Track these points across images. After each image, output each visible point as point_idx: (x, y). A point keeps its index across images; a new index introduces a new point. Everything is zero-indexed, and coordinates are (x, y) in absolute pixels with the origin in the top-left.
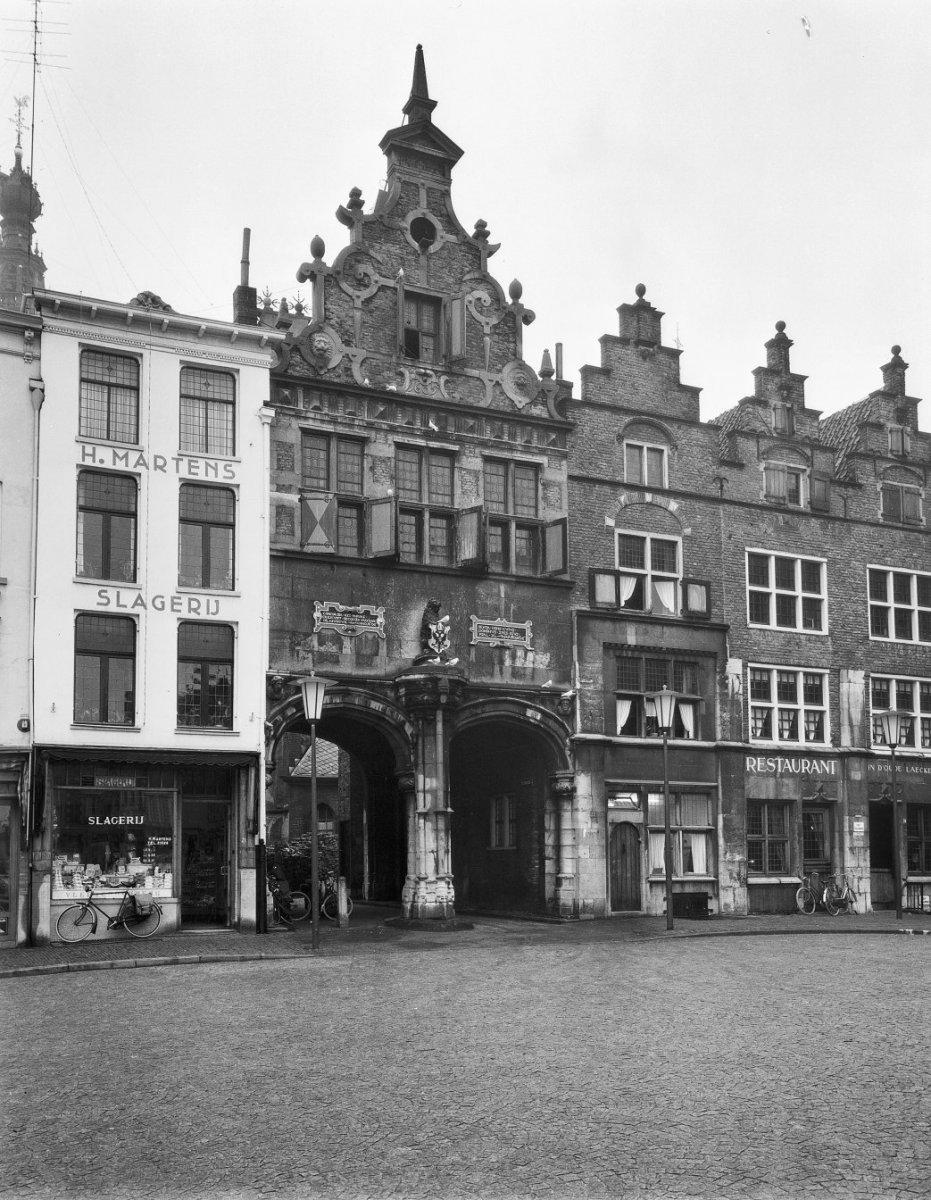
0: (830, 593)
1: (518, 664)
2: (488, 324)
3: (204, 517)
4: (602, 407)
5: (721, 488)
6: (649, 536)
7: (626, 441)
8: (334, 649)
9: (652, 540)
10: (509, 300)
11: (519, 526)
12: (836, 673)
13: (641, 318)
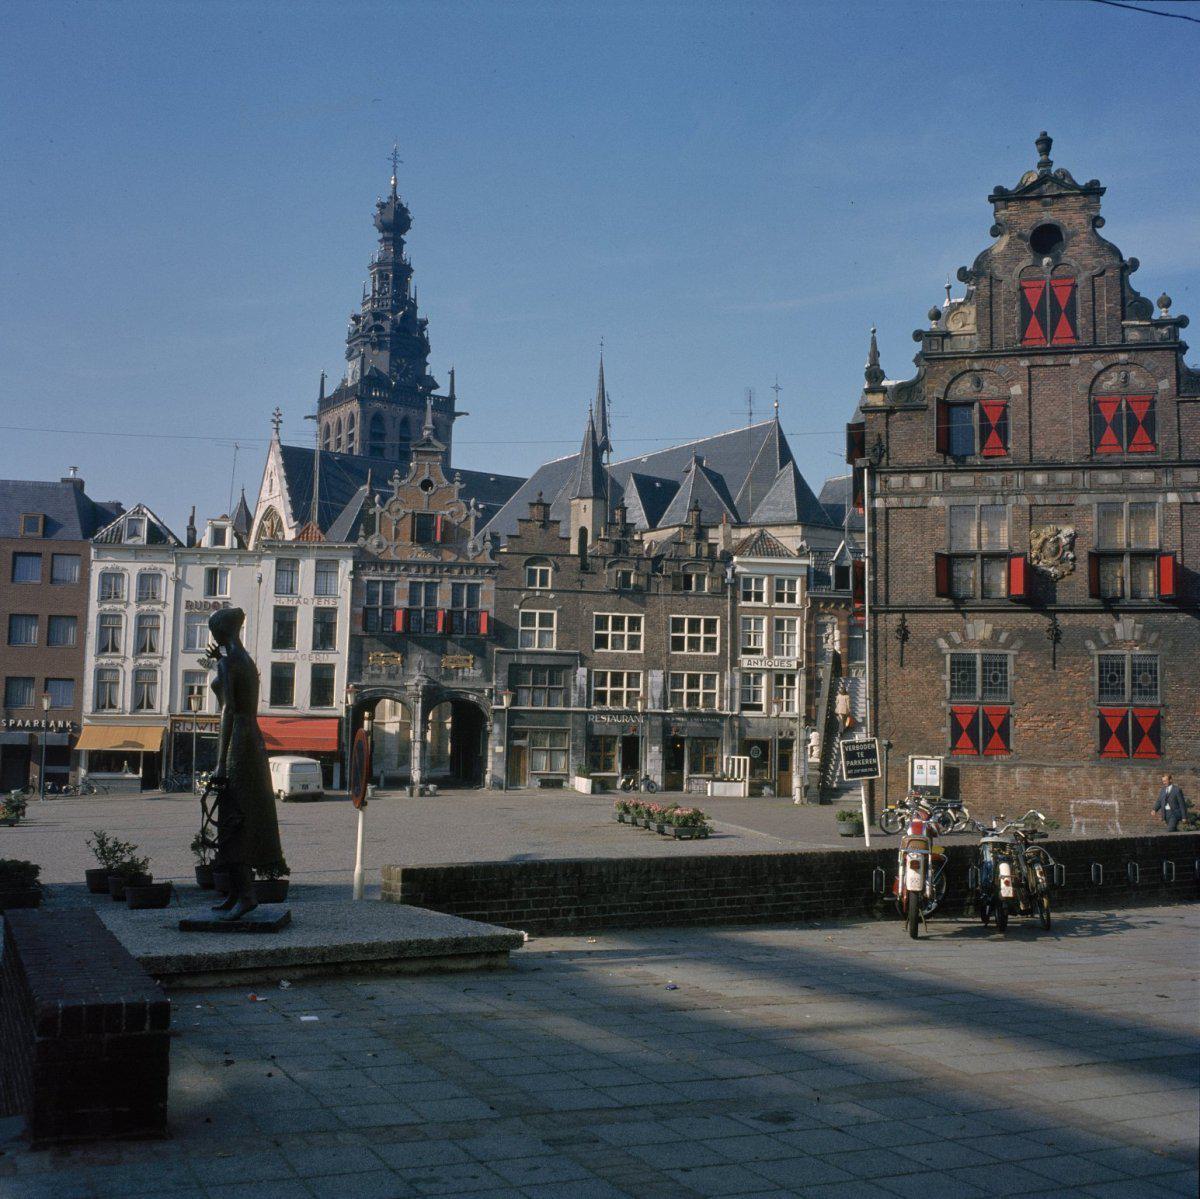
0: (645, 631)
1: (466, 674)
6: (538, 612)
8: (378, 672)
12: (646, 672)
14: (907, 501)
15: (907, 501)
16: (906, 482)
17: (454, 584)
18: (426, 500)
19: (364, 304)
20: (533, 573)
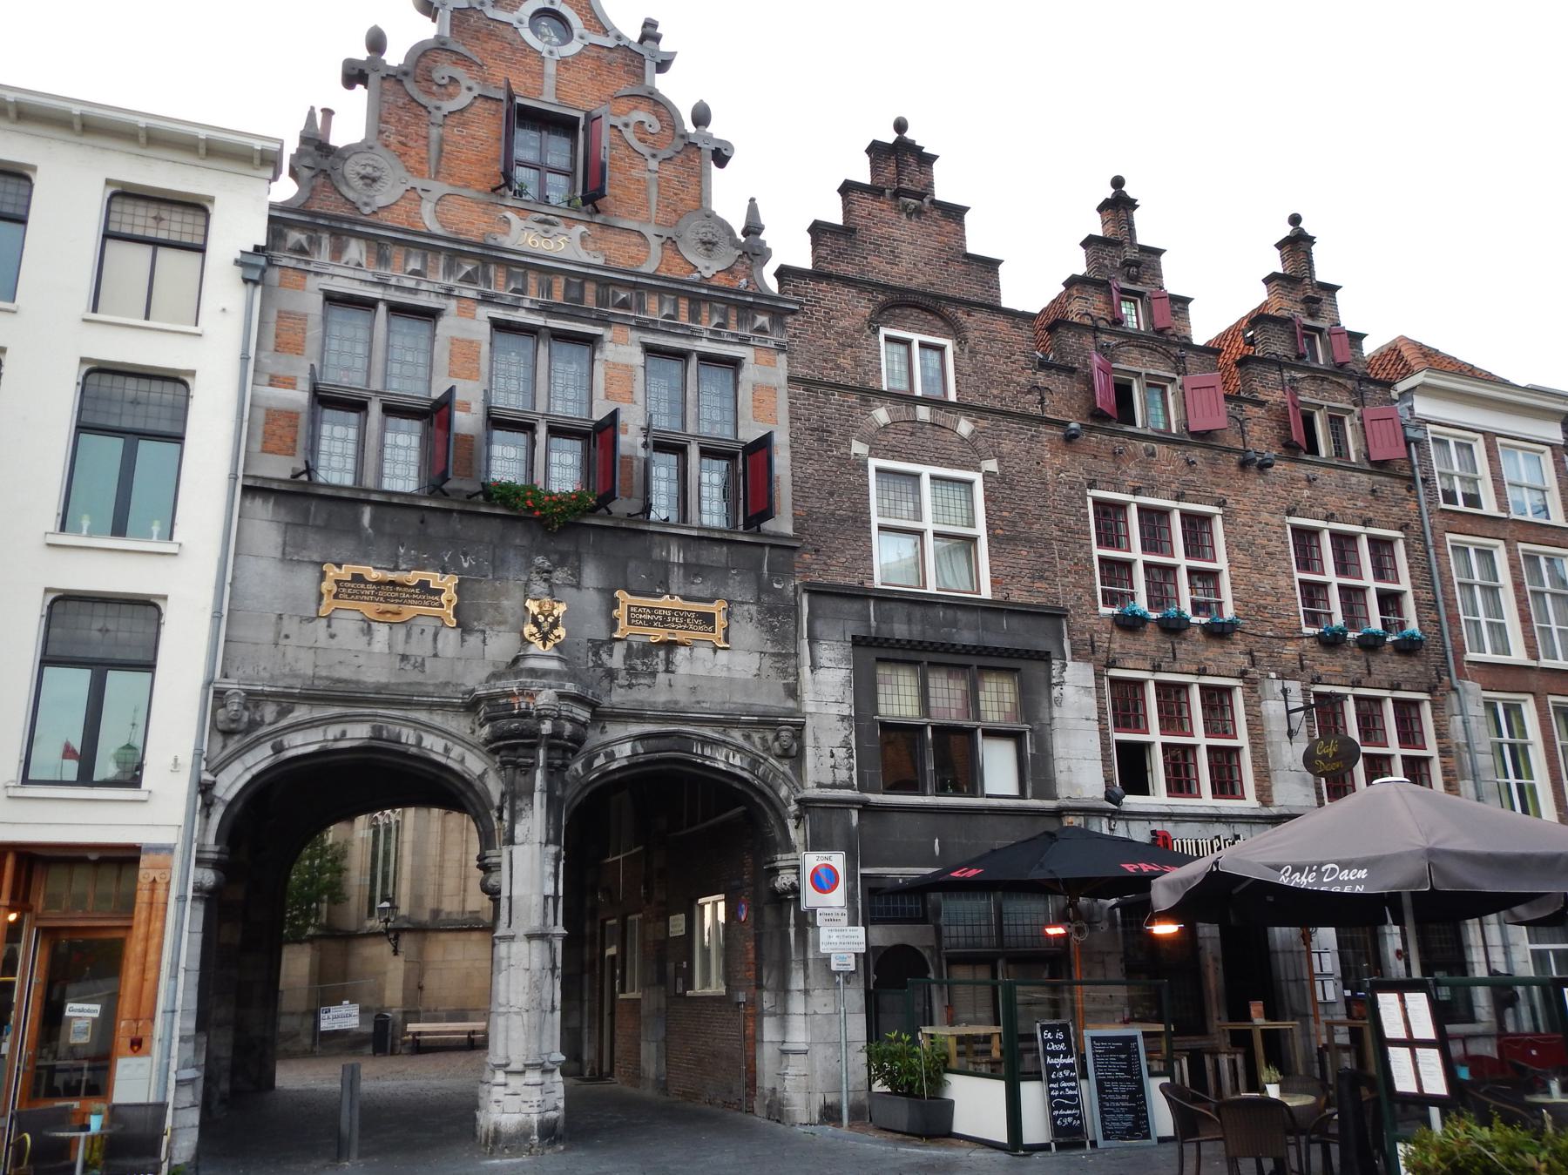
2: (654, 156)
3: (127, 423)
4: (847, 281)
5: (1042, 402)
6: (926, 471)
7: (883, 331)
9: (933, 478)
10: (690, 128)
11: (705, 452)
12: (1252, 685)
13: (900, 163)
17: (650, 350)
18: (550, 68)
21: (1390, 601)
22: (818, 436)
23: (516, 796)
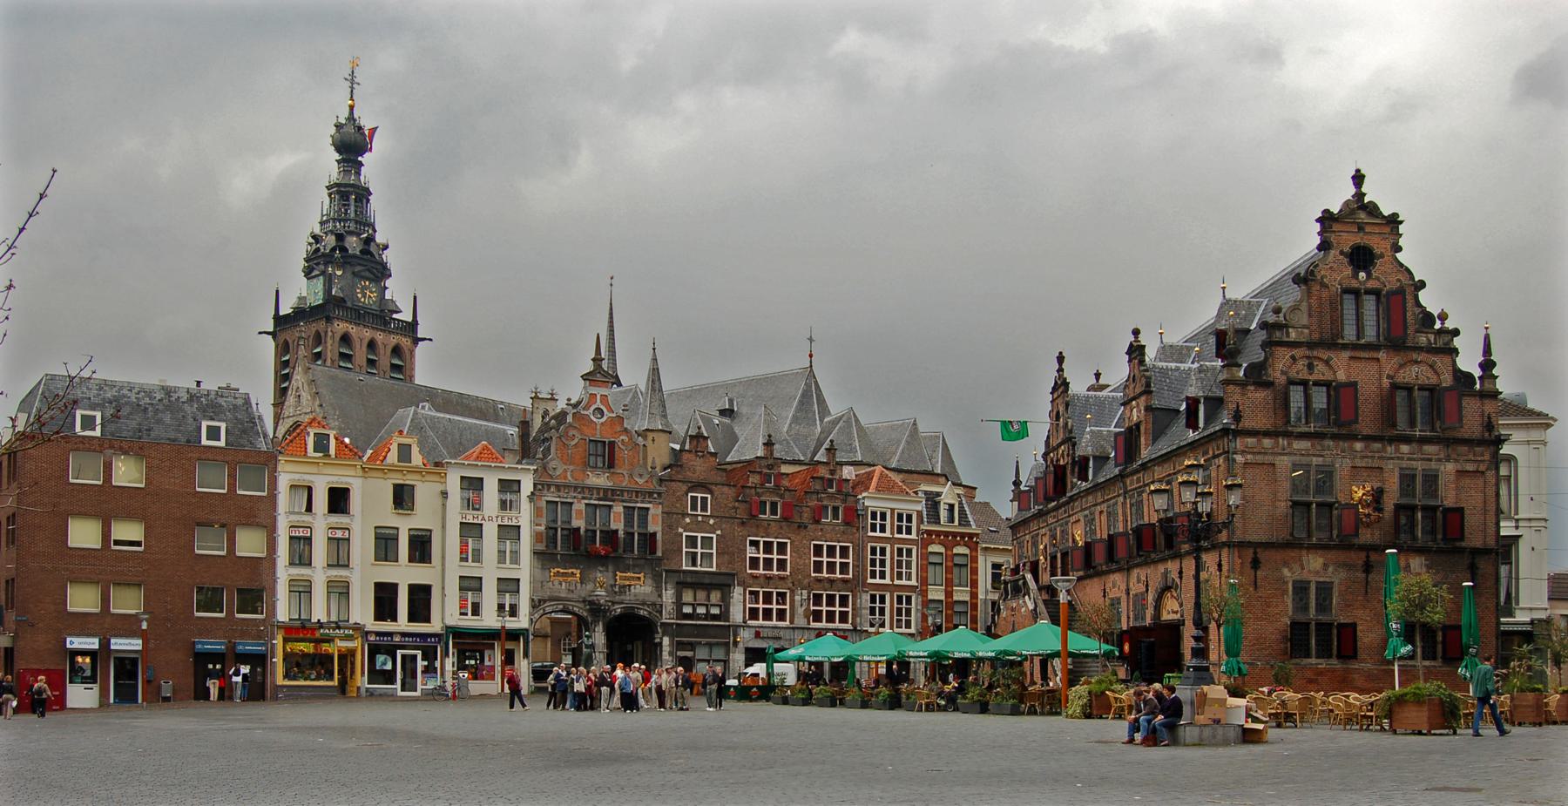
6: (699, 535)
12: (793, 592)
14: (1259, 458)
15: (1259, 458)
16: (1397, 450)
19: (322, 223)
20: (694, 499)
21: (844, 566)
22: (669, 527)
23: (595, 622)
